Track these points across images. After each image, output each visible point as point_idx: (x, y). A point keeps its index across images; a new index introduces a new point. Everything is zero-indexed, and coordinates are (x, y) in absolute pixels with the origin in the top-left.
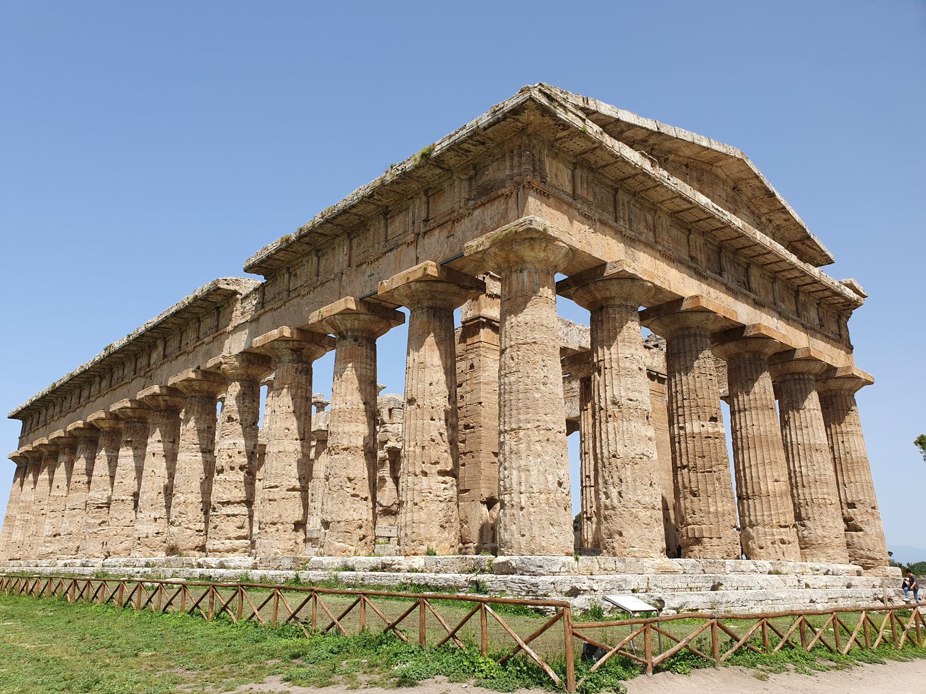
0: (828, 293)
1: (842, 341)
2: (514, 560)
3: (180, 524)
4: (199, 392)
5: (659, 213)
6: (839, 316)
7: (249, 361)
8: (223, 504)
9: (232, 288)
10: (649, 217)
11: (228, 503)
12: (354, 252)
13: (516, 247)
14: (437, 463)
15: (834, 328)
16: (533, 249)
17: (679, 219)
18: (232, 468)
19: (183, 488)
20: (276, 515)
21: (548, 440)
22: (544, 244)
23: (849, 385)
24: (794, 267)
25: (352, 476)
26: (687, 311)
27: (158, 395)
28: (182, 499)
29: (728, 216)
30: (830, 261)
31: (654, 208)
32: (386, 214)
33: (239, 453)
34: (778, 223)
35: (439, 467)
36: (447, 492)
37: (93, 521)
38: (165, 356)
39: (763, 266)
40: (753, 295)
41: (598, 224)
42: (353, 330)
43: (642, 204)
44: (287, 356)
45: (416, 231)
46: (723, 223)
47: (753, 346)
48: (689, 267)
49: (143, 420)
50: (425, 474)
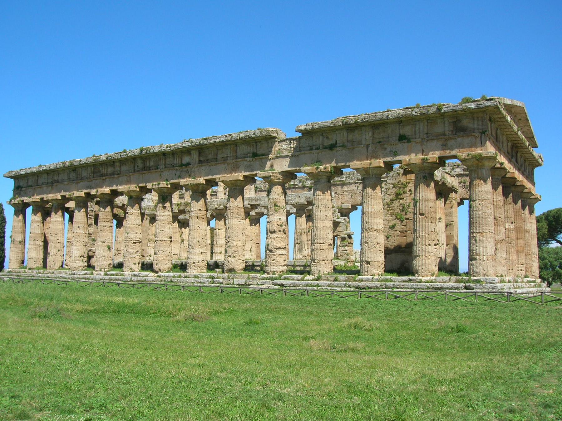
1: (530, 178)
2: (482, 278)
4: (239, 186)
7: (286, 176)
8: (277, 249)
9: (275, 135)
11: (279, 248)
12: (376, 136)
19: (235, 239)
30: (536, 147)
32: (400, 124)
38: (200, 161)
42: (375, 174)
44: (324, 179)
45: (422, 137)
50: (430, 245)
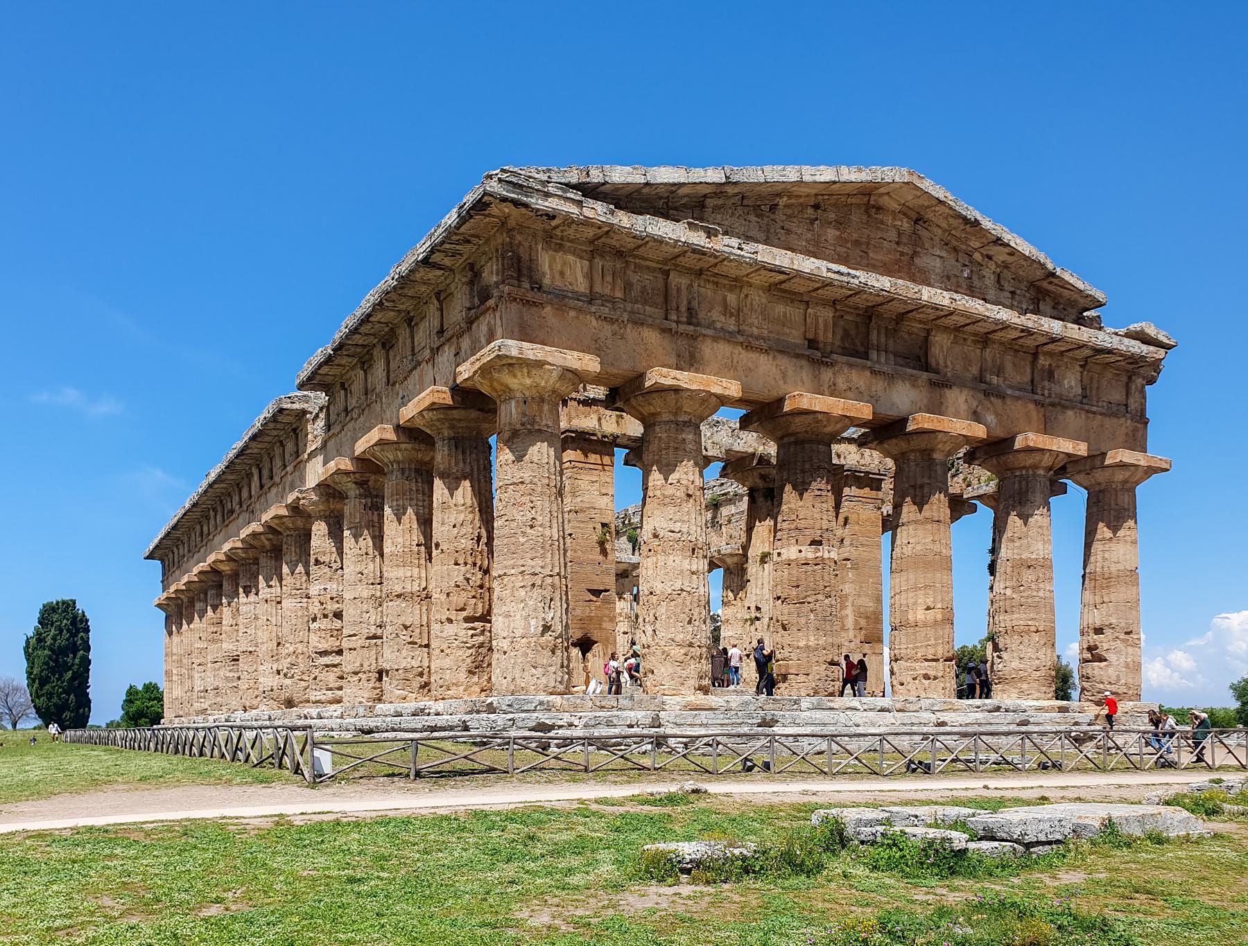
0: (1087, 352)
3: (293, 677)
5: (745, 291)
6: (1130, 378)
10: (732, 298)
13: (496, 375)
14: (463, 609)
15: (1116, 395)
16: (515, 376)
17: (785, 291)
18: (325, 616)
20: (358, 664)
21: (533, 585)
22: (525, 370)
23: (1120, 476)
24: (1005, 326)
25: (408, 624)
26: (787, 414)
27: (260, 534)
28: (291, 649)
29: (863, 277)
31: (737, 283)
33: (332, 598)
34: (1002, 258)
35: (465, 614)
36: (475, 638)
37: (231, 674)
39: (958, 329)
40: (925, 375)
41: (630, 326)
43: (717, 284)
46: (850, 289)
47: (917, 443)
48: (798, 356)
49: (256, 561)
50: (450, 621)
